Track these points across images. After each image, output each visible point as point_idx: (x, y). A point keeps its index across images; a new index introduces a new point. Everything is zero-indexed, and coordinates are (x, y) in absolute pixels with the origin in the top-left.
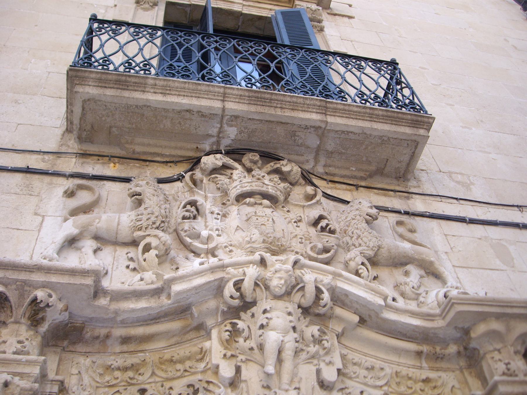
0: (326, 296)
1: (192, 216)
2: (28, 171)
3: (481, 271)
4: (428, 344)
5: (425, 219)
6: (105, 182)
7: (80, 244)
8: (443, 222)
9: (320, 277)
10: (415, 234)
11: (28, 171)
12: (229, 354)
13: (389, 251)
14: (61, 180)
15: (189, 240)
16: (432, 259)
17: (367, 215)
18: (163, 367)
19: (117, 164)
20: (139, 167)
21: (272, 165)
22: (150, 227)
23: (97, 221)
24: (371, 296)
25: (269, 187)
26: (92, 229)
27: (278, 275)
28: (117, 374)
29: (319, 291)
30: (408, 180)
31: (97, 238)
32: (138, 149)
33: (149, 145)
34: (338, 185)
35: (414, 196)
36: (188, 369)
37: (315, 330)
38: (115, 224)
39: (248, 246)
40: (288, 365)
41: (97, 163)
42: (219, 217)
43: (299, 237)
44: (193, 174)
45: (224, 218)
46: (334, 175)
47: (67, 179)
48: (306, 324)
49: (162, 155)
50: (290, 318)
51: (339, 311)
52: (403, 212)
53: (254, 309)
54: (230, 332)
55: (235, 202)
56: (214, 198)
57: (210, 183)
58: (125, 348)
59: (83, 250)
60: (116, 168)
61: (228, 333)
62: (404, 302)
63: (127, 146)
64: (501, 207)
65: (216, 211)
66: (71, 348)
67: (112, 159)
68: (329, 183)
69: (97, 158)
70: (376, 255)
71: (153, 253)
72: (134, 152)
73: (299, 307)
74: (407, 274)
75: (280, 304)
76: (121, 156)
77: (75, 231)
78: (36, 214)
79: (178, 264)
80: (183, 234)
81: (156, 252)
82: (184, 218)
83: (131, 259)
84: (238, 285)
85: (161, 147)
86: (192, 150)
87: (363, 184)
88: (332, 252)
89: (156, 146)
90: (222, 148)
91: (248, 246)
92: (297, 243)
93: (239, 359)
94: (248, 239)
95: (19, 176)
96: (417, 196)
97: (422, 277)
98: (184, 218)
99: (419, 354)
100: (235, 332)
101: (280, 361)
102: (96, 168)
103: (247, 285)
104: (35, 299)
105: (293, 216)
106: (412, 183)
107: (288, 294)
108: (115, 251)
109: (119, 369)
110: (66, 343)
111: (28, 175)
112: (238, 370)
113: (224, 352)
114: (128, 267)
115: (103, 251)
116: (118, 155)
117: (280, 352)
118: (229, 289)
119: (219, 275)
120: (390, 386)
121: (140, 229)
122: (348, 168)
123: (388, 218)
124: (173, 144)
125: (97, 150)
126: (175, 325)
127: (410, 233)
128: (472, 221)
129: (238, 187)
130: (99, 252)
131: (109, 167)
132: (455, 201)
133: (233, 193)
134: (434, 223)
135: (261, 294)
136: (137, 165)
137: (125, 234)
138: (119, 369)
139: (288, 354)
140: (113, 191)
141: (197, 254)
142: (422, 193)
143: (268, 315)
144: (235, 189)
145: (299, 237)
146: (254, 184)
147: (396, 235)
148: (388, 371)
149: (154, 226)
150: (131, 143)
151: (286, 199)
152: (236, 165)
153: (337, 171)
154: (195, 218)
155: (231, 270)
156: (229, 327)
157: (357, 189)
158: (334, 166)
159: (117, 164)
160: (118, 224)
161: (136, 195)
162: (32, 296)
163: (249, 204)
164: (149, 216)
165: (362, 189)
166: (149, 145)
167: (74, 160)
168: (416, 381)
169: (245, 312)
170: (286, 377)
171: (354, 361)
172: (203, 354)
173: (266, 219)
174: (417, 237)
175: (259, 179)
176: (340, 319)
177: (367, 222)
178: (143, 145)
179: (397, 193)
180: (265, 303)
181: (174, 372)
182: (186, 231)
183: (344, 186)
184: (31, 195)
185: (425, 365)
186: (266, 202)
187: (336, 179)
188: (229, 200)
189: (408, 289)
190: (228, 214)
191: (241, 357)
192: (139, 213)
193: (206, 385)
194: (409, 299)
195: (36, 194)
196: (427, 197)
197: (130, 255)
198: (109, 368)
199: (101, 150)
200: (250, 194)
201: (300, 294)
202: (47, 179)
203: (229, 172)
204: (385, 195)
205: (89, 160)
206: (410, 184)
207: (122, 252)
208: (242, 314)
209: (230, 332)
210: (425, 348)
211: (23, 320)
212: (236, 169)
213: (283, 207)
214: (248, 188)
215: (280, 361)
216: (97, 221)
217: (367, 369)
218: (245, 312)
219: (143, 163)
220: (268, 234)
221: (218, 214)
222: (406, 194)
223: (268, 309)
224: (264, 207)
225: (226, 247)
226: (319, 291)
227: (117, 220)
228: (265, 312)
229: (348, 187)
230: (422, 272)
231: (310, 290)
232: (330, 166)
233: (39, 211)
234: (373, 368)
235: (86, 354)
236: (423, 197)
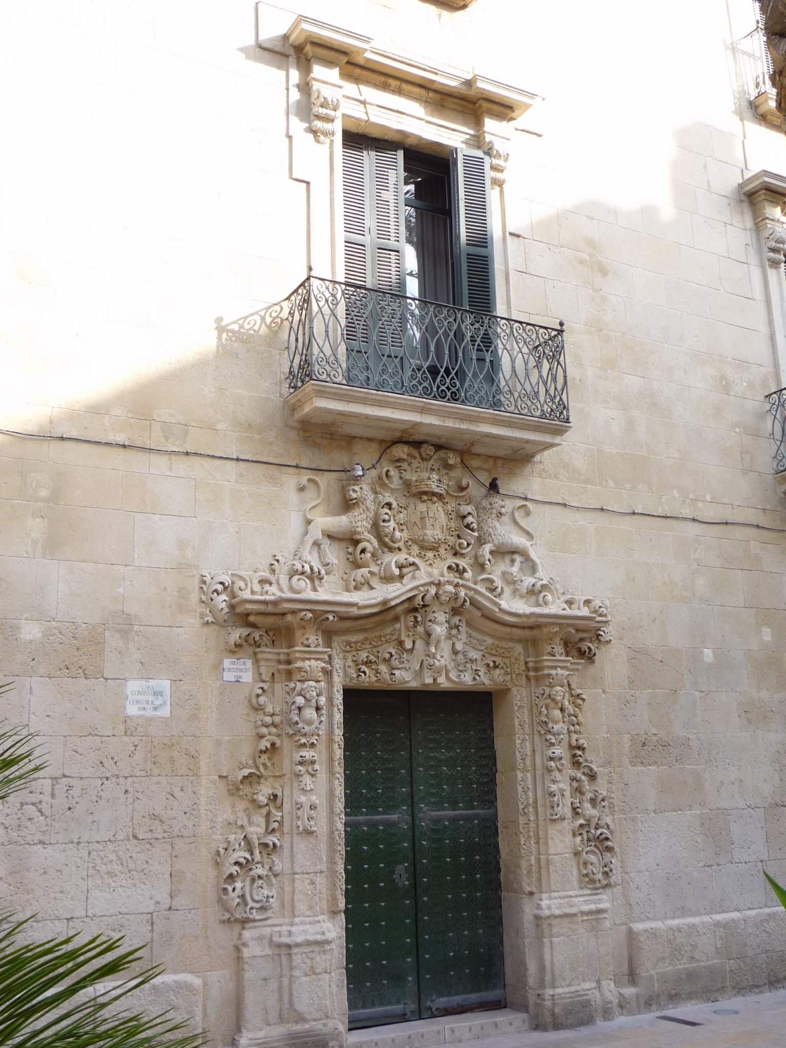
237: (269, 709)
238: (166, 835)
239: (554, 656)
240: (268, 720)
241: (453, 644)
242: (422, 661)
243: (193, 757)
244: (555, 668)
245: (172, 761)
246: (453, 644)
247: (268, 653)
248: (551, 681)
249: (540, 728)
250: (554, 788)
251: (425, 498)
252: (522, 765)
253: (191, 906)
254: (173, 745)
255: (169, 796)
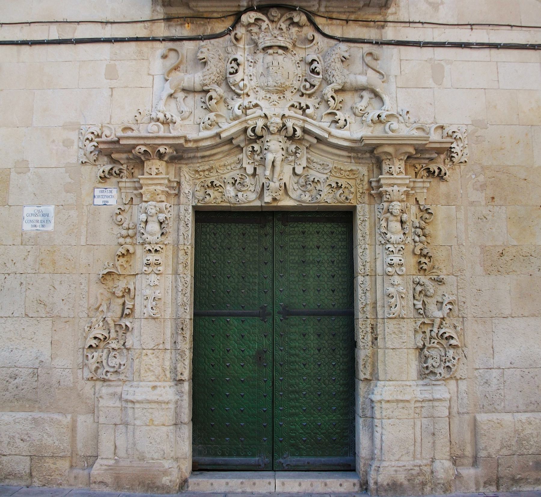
0: (299, 133)
1: (235, 71)
2: (137, 39)
3: (415, 89)
4: (354, 153)
5: (390, 46)
6: (184, 42)
7: (176, 95)
8: (402, 48)
9: (296, 122)
10: (379, 62)
11: (137, 39)
12: (250, 163)
13: (351, 84)
14: (157, 44)
15: (233, 88)
16: (377, 90)
17: (343, 57)
18: (221, 168)
19: (190, 24)
20: (203, 25)
21: (287, 15)
22: (211, 83)
23: (182, 82)
24: (322, 132)
25: (282, 42)
26: (181, 87)
27: (273, 125)
28: (201, 173)
29: (295, 130)
30: (388, 8)
31: (184, 90)
32: (201, 10)
33: (207, 7)
34: (335, 22)
35: (389, 24)
36: (233, 168)
37: (293, 148)
38: (193, 84)
39: (266, 88)
40: (278, 169)
41: (178, 25)
42: (252, 64)
43: (298, 76)
44: (236, 34)
45: (255, 64)
46: (333, 12)
47: (162, 43)
48: (290, 143)
49: (218, 12)
50: (280, 144)
51: (307, 137)
52: (374, 42)
53: (262, 139)
54: (251, 151)
55: (262, 51)
56: (249, 48)
57: (248, 33)
58: (203, 160)
59: (178, 100)
60: (189, 28)
61: (250, 152)
62: (355, 118)
63: (194, 9)
64: (456, 27)
65: (250, 58)
66: (179, 162)
67: (186, 19)
68: (328, 20)
69: (176, 20)
70: (343, 87)
71: (214, 101)
72: (199, 12)
73: (285, 137)
74: (362, 97)
75: (276, 137)
76: (191, 16)
77: (172, 92)
78: (149, 74)
79: (228, 103)
80: (230, 84)
81: (215, 101)
82: (231, 74)
83: (204, 102)
84: (253, 130)
85: (216, 7)
86: (236, 6)
87: (353, 17)
88: (315, 88)
89: (212, 6)
90: (255, 4)
91: (266, 88)
92: (296, 81)
93: (255, 164)
94: (266, 84)
95: (133, 44)
96: (391, 24)
97: (371, 98)
98: (231, 74)
99: (350, 157)
100: (253, 151)
101: (273, 166)
102: (177, 30)
103: (258, 131)
104: (159, 150)
105: (297, 58)
106: (392, 10)
107: (279, 131)
108: (195, 96)
109: (201, 171)
110: (176, 161)
111: (139, 43)
112: (255, 169)
113: (248, 161)
114: (202, 107)
115: (188, 97)
116: (190, 15)
117: (273, 162)
118: (249, 132)
119: (244, 125)
120: (331, 173)
121: (206, 85)
122: (342, 7)
123: (362, 49)
124: (223, 4)
125: (176, 12)
126: (226, 148)
127: (375, 61)
128: (426, 44)
129: (262, 43)
130: (186, 98)
131: (185, 27)
132: (420, 25)
133: (261, 46)
134: (395, 50)
135: (264, 133)
136: (202, 22)
137: (198, 87)
138: (201, 171)
139: (278, 163)
140: (190, 49)
141: (239, 95)
142: (396, 21)
143: (269, 144)
144: (261, 44)
145: (298, 76)
146: (271, 41)
147: (364, 64)
148: (331, 166)
149: (214, 82)
150: (196, 7)
151: (294, 45)
152: (264, 18)
153: (335, 10)
154: (237, 71)
155: (249, 122)
156: (251, 149)
157: (347, 23)
158: (333, 7)
159: (190, 24)
160: (194, 83)
161: (202, 59)
162: (158, 150)
163: (270, 54)
164: (210, 76)
165: (351, 22)
166: (207, 7)
167: (163, 24)
168: (345, 171)
169: (259, 140)
170: (276, 175)
171: (314, 161)
172: (240, 161)
173: (278, 67)
174: (378, 65)
175: (275, 37)
176: (308, 141)
177: (342, 61)
178: (204, 7)
179: (377, 23)
180: (268, 138)
181: (226, 170)
182: (231, 83)
183: (338, 21)
184: (143, 59)
185: (353, 161)
186: (280, 51)
187: (334, 16)
188: (258, 50)
189: (357, 112)
190: (257, 61)
191: (256, 163)
192: (205, 74)
193: (240, 177)
194: (358, 116)
195: (146, 58)
196: (399, 24)
197: (203, 100)
198: (197, 171)
199: (179, 12)
200: (270, 47)
201: (285, 132)
202: (150, 44)
203: (260, 22)
204: (367, 26)
205: (172, 23)
206: (390, 11)
207: (198, 96)
208: (258, 141)
209: (251, 151)
210: (352, 155)
211: (155, 157)
212: (264, 21)
213: (292, 51)
214: (268, 44)
215: (273, 166)
216: (182, 82)
217: (320, 165)
218: (259, 140)
219: (206, 21)
220: (277, 81)
221: (252, 62)
222: (382, 23)
223: (269, 140)
224: (279, 55)
225: (255, 88)
226: (295, 130)
227: (193, 80)
228: (267, 141)
229: (341, 22)
230: (372, 96)
231: (291, 131)
232: (329, 7)
233: (151, 72)
234: (323, 164)
235: (186, 164)
236: (396, 24)
237: (125, 225)
238: (48, 315)
239: (393, 175)
240: (124, 233)
241: (294, 169)
242: (263, 184)
243: (69, 260)
244: (392, 185)
245: (54, 263)
246: (294, 169)
247: (126, 182)
248: (388, 196)
249: (381, 239)
250: (391, 290)
251: (270, 51)
252: (363, 270)
253: (65, 367)
254: (55, 251)
255: (51, 288)
